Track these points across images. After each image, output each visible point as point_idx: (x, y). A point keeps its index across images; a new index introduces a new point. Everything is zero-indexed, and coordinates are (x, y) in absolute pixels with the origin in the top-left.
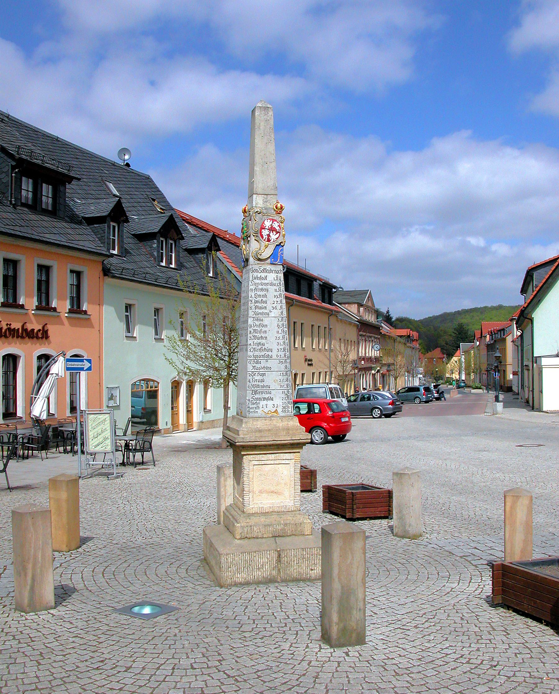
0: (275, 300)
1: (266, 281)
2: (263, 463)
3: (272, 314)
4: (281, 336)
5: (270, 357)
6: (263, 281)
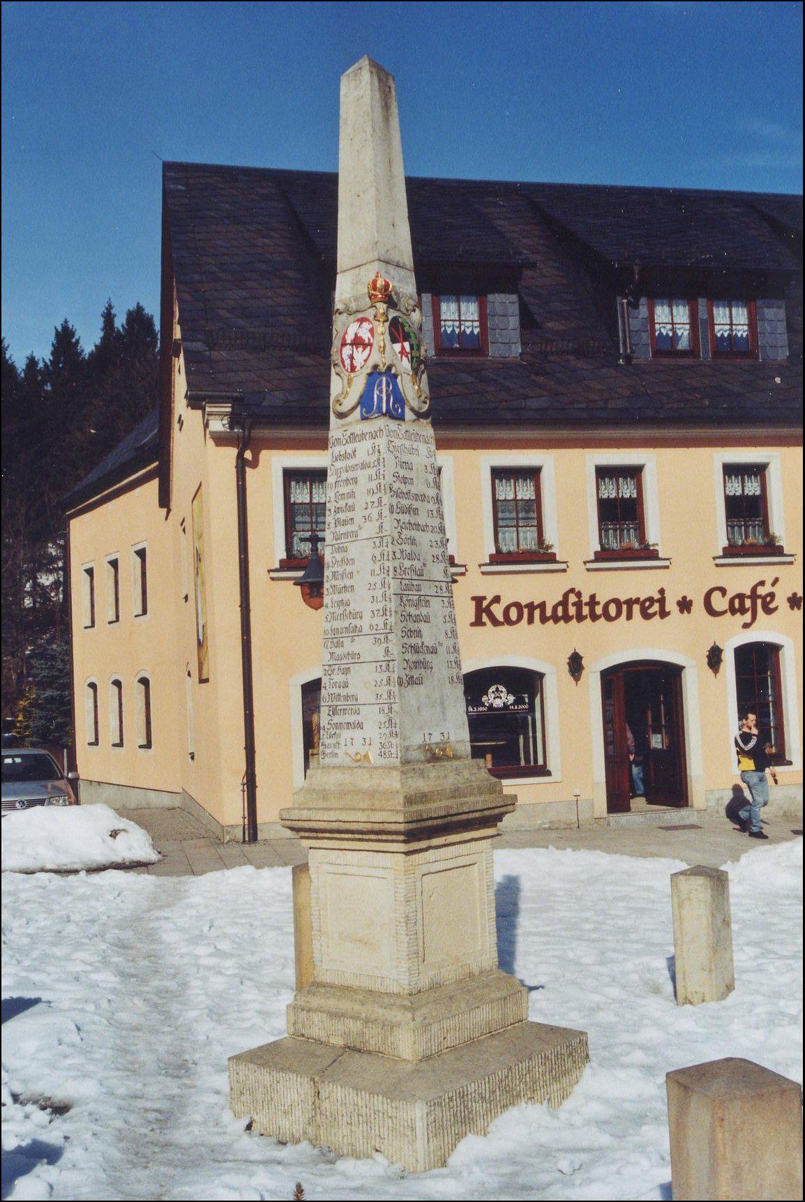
0: (370, 499)
1: (351, 462)
2: (341, 869)
3: (363, 534)
4: (378, 580)
5: (357, 630)
6: (351, 462)
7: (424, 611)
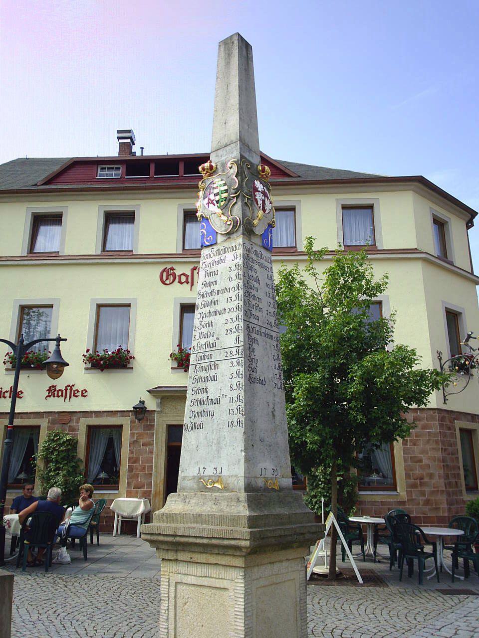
7: (212, 373)
